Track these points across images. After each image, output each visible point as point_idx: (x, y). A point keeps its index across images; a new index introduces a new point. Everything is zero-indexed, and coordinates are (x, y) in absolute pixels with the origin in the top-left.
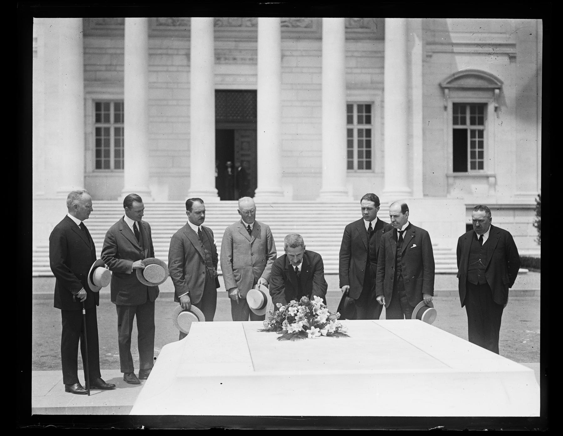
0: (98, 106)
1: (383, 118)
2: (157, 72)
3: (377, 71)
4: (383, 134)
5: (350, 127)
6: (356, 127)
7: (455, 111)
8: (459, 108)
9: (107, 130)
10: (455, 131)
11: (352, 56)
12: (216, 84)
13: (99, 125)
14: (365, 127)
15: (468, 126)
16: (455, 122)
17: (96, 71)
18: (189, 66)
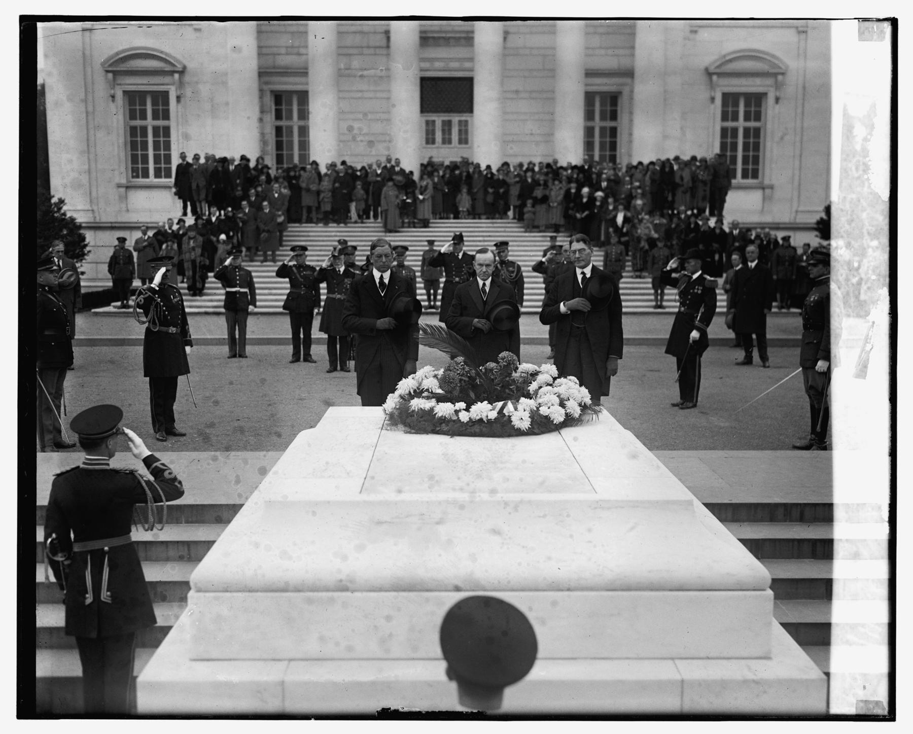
0: (278, 97)
1: (631, 113)
2: (350, 55)
3: (627, 52)
4: (631, 134)
5: (590, 124)
6: (598, 123)
7: (725, 103)
8: (730, 100)
9: (290, 129)
10: (724, 131)
11: (595, 33)
12: (421, 70)
13: (279, 123)
14: (609, 124)
15: (741, 124)
16: (724, 118)
17: (274, 55)
18: (388, 47)
